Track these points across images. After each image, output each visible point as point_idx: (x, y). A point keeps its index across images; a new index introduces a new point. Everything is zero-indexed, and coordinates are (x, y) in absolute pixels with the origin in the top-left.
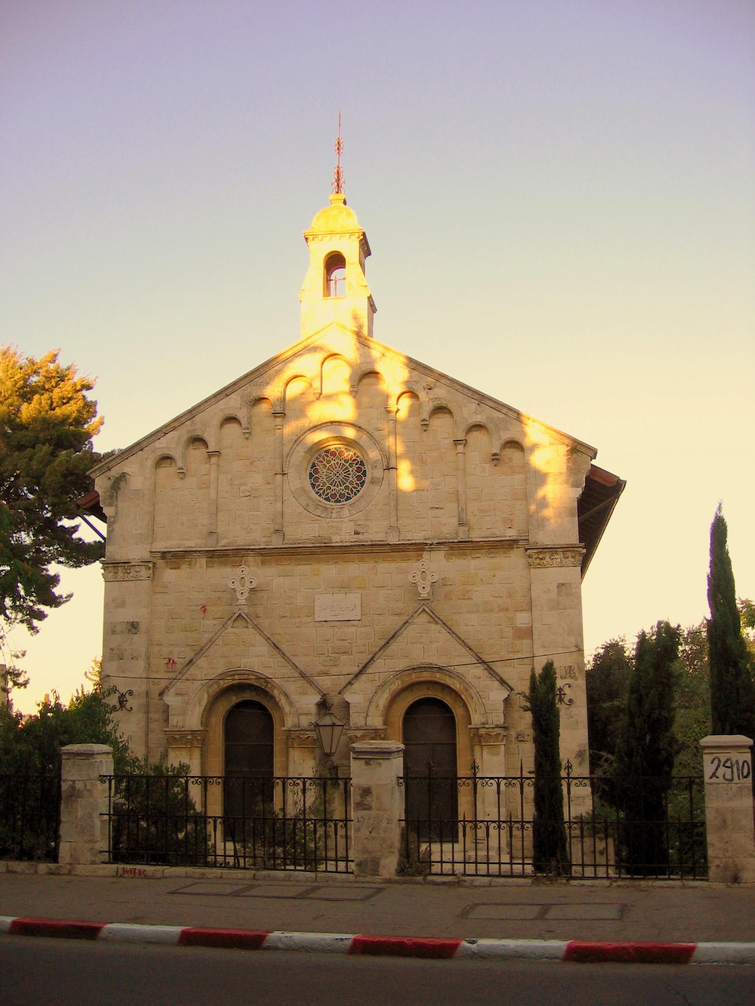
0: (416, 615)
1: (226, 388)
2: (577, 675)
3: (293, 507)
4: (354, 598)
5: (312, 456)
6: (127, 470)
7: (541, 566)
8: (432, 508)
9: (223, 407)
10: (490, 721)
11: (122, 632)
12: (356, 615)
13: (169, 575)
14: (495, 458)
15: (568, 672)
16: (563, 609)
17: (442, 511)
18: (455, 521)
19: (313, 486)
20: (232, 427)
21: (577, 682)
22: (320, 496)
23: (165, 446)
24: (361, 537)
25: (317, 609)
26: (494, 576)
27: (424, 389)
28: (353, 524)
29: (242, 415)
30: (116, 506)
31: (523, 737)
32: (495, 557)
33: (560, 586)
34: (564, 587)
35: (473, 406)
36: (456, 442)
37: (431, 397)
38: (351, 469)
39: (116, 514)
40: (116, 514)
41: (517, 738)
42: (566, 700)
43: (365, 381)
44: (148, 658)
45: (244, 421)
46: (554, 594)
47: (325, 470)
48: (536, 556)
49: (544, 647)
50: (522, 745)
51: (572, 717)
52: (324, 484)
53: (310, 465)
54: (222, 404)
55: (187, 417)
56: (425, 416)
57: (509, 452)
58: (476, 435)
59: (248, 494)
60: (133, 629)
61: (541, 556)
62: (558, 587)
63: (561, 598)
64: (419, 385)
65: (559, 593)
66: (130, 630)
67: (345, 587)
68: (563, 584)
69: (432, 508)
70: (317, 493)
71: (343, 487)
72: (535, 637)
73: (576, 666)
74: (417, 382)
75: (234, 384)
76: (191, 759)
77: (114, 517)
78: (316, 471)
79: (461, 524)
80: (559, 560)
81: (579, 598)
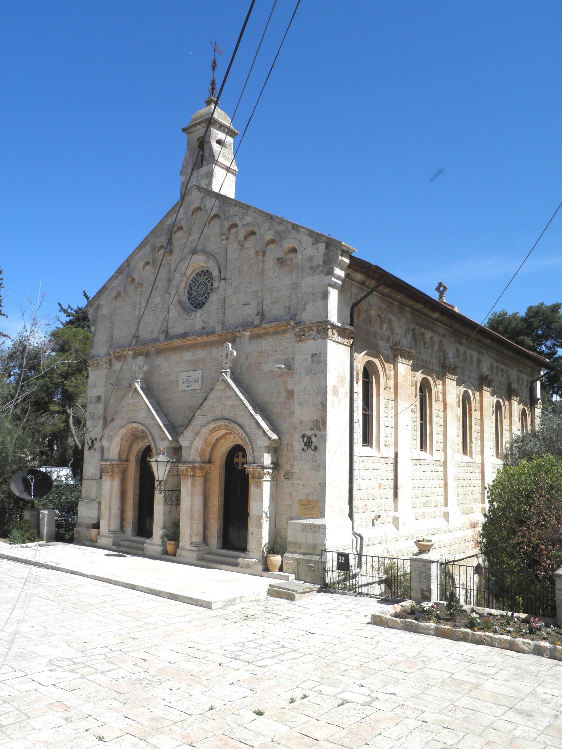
0: (218, 383)
1: (142, 243)
2: (321, 427)
3: (174, 313)
4: (198, 374)
5: (188, 279)
6: (101, 302)
7: (300, 340)
8: (244, 305)
9: (142, 254)
10: (256, 462)
11: (94, 402)
12: (198, 386)
13: (117, 366)
14: (281, 261)
15: (315, 424)
16: (314, 374)
17: (249, 306)
18: (255, 312)
19: (189, 298)
20: (148, 267)
21: (321, 433)
22: (192, 305)
23: (116, 285)
24: (204, 330)
25: (180, 382)
26: (276, 351)
27: (240, 219)
28: (201, 322)
29: (150, 259)
30: (96, 325)
31: (288, 475)
32: (278, 337)
33: (314, 355)
34: (316, 357)
35: (267, 225)
36: (257, 253)
37: (244, 224)
38: (208, 284)
39: (96, 330)
40: (96, 330)
41: (284, 476)
42: (313, 447)
43: (212, 222)
44: (105, 418)
45: (151, 262)
46: (309, 362)
47: (195, 287)
48: (298, 334)
49: (301, 405)
50: (287, 482)
51: (316, 461)
52: (195, 297)
53: (188, 285)
54: (141, 253)
55: (126, 264)
56: (241, 238)
57: (291, 255)
58: (271, 246)
59: (153, 309)
60: (99, 401)
61: (302, 333)
62: (312, 356)
63: (314, 365)
64: (237, 217)
65: (312, 362)
66: (97, 401)
67: (195, 365)
68: (315, 354)
69: (244, 305)
70: (191, 303)
71: (204, 298)
72: (295, 396)
73: (321, 420)
74: (236, 215)
75: (146, 238)
76: (113, 481)
77: (95, 332)
78: (191, 289)
79: (258, 314)
80: (314, 335)
81: (326, 364)
